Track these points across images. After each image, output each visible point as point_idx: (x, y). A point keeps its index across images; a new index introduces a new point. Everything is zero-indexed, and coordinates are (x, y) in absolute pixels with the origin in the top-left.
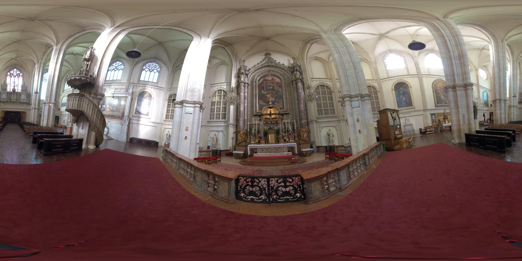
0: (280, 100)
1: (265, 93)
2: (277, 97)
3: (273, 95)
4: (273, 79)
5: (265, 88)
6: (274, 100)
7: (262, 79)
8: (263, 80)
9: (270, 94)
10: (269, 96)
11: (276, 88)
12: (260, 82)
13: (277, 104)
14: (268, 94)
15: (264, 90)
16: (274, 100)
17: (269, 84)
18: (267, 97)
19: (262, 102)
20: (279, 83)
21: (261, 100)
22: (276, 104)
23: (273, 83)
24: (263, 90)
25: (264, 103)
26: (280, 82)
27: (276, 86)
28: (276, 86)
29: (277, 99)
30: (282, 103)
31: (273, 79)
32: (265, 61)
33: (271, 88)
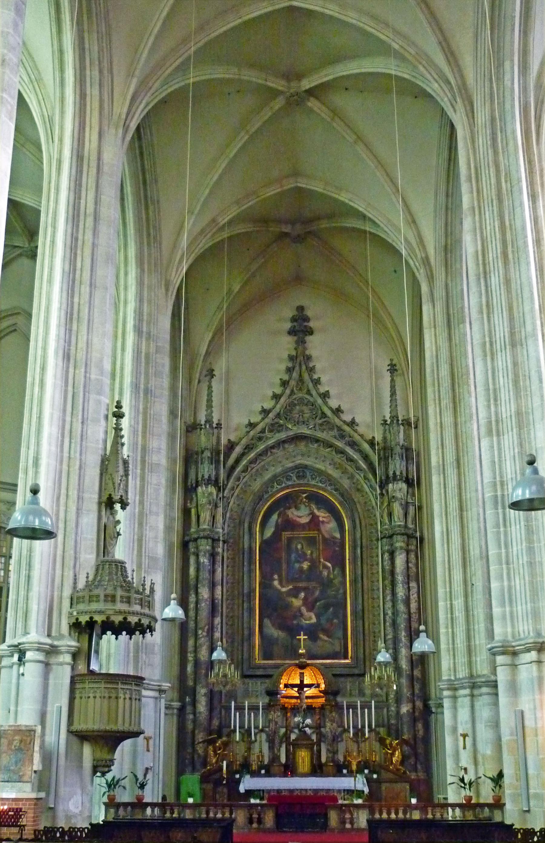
0: (335, 621)
1: (284, 590)
2: (326, 607)
3: (310, 599)
4: (314, 522)
5: (284, 566)
6: (314, 620)
7: (275, 517)
8: (277, 521)
9: (302, 595)
10: (297, 602)
11: (325, 567)
12: (269, 532)
13: (325, 638)
14: (295, 593)
15: (280, 576)
16: (314, 620)
17: (299, 546)
18: (288, 606)
19: (273, 625)
20: (335, 543)
21: (269, 617)
22: (321, 636)
23: (312, 541)
24: (276, 577)
25: (280, 633)
26: (338, 535)
27: (322, 560)
28: (322, 560)
29: (325, 617)
30: (340, 634)
31: (314, 522)
32: (283, 400)
33: (305, 565)
